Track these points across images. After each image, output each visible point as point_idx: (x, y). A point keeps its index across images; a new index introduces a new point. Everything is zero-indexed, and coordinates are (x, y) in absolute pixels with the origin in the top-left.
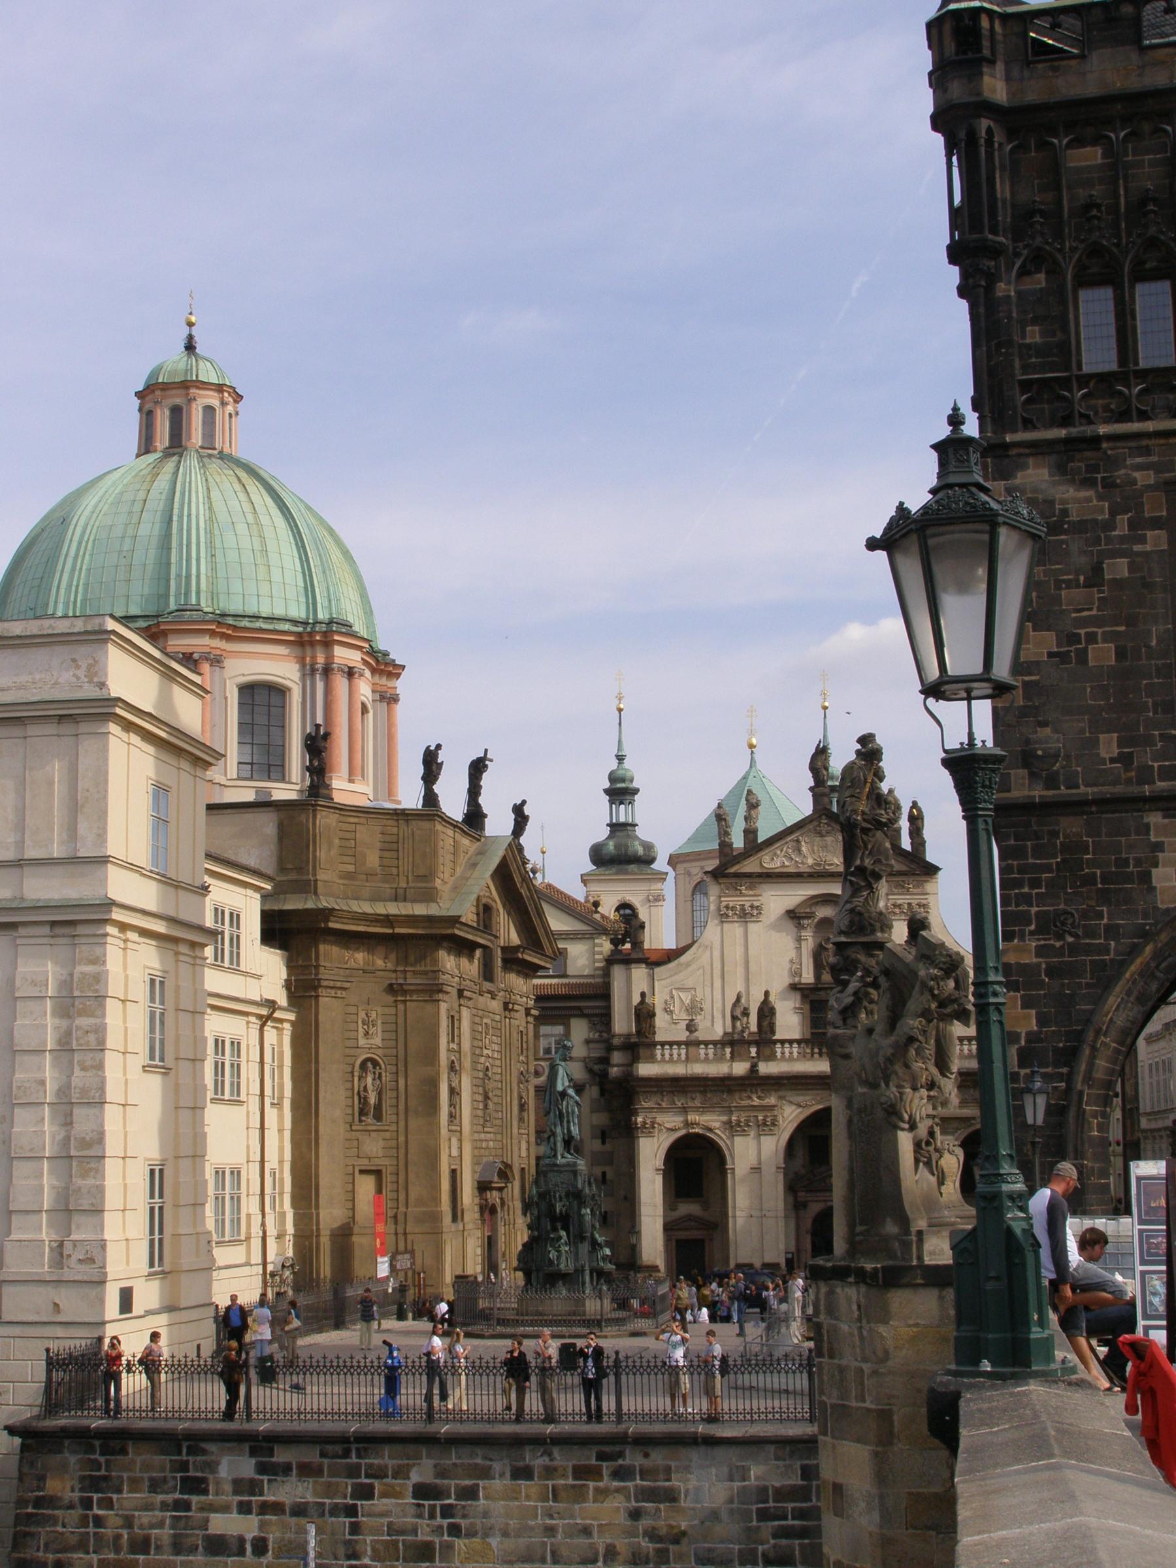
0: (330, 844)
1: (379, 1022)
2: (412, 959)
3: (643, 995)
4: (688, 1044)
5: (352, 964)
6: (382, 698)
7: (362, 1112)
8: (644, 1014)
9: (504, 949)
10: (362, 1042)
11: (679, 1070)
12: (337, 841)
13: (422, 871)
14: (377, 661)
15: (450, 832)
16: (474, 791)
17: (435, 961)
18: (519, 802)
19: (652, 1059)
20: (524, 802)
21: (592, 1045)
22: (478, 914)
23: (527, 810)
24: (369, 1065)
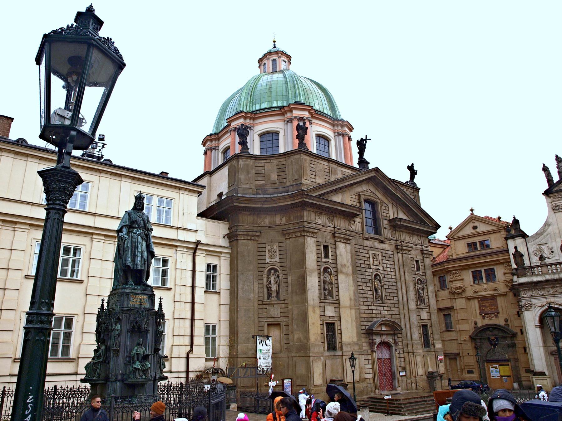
0: (248, 173)
1: (278, 250)
2: (292, 218)
3: (516, 248)
4: (541, 266)
5: (263, 224)
6: (339, 135)
7: (269, 295)
8: (518, 255)
9: (390, 221)
10: (268, 260)
11: (539, 279)
12: (254, 171)
13: (296, 177)
14: (334, 121)
15: (326, 164)
16: (361, 152)
17: (302, 217)
18: (410, 165)
19: (525, 275)
20: (413, 164)
21: (506, 275)
22: (360, 203)
23: (415, 168)
24: (272, 271)
